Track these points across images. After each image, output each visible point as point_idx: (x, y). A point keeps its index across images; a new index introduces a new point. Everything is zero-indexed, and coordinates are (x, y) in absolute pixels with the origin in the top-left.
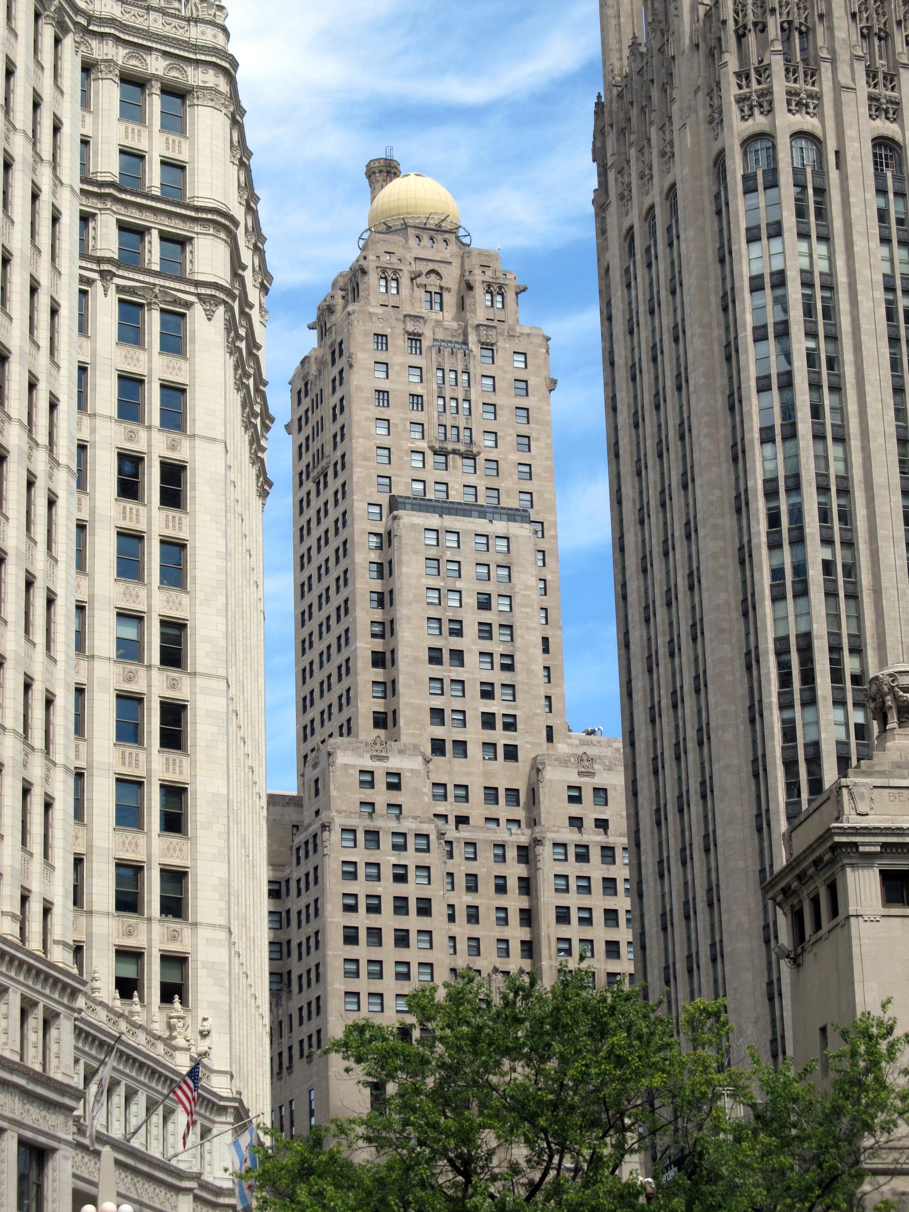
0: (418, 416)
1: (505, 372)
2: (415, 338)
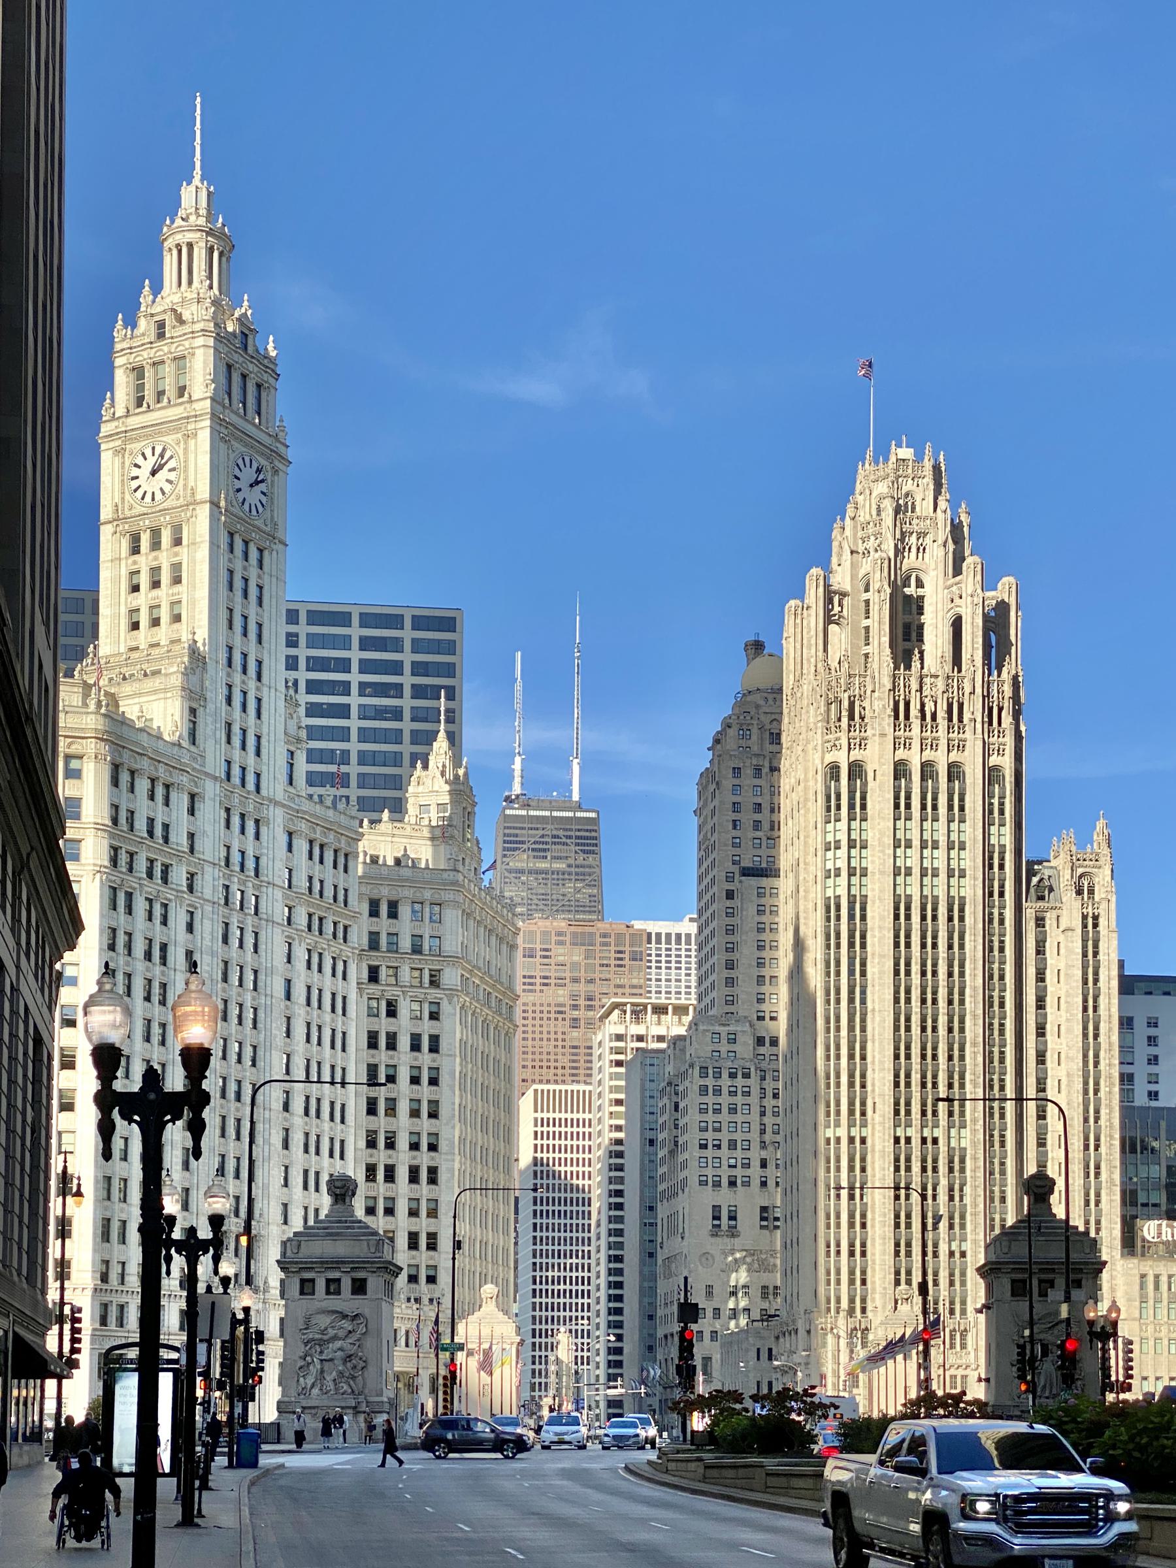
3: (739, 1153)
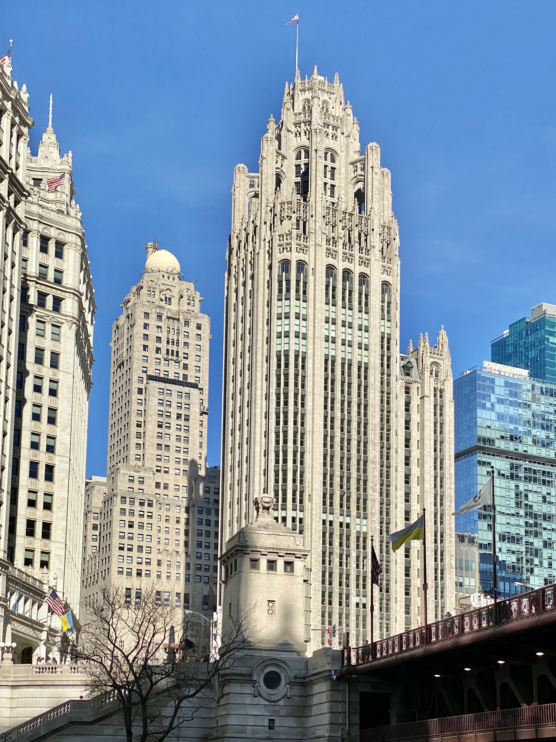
0: (159, 345)
1: (193, 331)
2: (159, 317)
3: (144, 555)
